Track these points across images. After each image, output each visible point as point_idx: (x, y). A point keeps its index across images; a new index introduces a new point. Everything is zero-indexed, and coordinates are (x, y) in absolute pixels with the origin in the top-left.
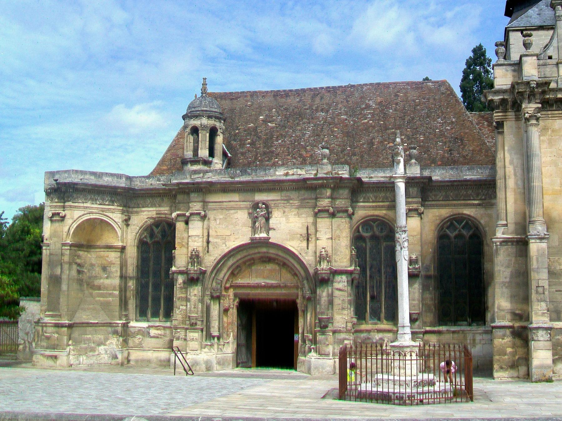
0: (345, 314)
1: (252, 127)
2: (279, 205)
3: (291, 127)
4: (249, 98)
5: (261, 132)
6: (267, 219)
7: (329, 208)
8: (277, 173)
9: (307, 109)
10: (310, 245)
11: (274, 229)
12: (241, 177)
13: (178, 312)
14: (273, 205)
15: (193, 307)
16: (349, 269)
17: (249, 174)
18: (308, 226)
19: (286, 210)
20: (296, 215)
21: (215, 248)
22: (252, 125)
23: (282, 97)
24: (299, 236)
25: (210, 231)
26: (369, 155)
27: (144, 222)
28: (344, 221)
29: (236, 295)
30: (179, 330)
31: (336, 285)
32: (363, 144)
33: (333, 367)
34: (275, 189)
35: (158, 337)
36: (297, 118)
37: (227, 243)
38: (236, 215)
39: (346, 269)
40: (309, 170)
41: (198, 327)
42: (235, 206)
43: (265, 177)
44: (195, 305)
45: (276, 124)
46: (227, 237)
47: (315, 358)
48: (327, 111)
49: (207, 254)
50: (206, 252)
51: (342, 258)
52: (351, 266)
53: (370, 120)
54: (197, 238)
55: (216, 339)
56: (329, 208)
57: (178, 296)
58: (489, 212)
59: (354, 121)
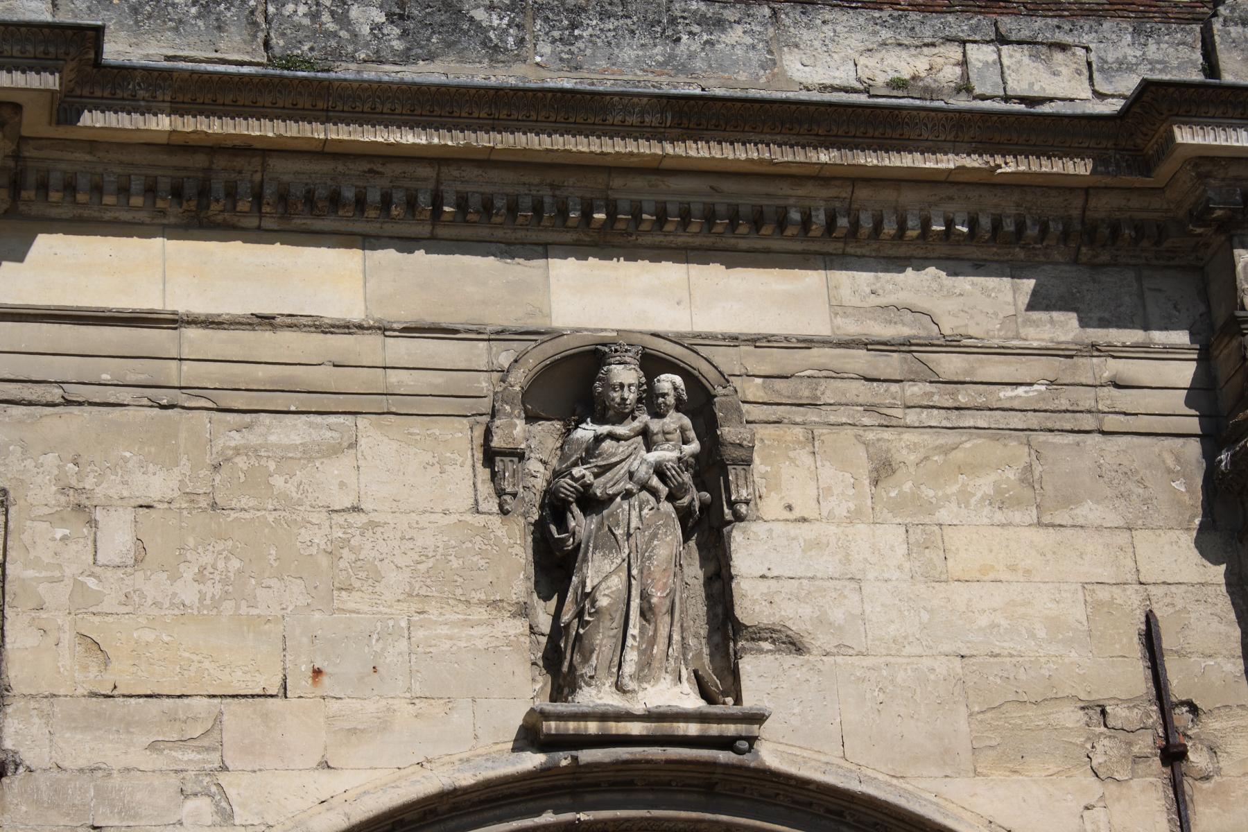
2: (830, 391)
11: (795, 646)
14: (753, 389)
18: (1150, 619)
19: (904, 447)
20: (1017, 503)
24: (1071, 718)
34: (782, 223)
38: (336, 469)
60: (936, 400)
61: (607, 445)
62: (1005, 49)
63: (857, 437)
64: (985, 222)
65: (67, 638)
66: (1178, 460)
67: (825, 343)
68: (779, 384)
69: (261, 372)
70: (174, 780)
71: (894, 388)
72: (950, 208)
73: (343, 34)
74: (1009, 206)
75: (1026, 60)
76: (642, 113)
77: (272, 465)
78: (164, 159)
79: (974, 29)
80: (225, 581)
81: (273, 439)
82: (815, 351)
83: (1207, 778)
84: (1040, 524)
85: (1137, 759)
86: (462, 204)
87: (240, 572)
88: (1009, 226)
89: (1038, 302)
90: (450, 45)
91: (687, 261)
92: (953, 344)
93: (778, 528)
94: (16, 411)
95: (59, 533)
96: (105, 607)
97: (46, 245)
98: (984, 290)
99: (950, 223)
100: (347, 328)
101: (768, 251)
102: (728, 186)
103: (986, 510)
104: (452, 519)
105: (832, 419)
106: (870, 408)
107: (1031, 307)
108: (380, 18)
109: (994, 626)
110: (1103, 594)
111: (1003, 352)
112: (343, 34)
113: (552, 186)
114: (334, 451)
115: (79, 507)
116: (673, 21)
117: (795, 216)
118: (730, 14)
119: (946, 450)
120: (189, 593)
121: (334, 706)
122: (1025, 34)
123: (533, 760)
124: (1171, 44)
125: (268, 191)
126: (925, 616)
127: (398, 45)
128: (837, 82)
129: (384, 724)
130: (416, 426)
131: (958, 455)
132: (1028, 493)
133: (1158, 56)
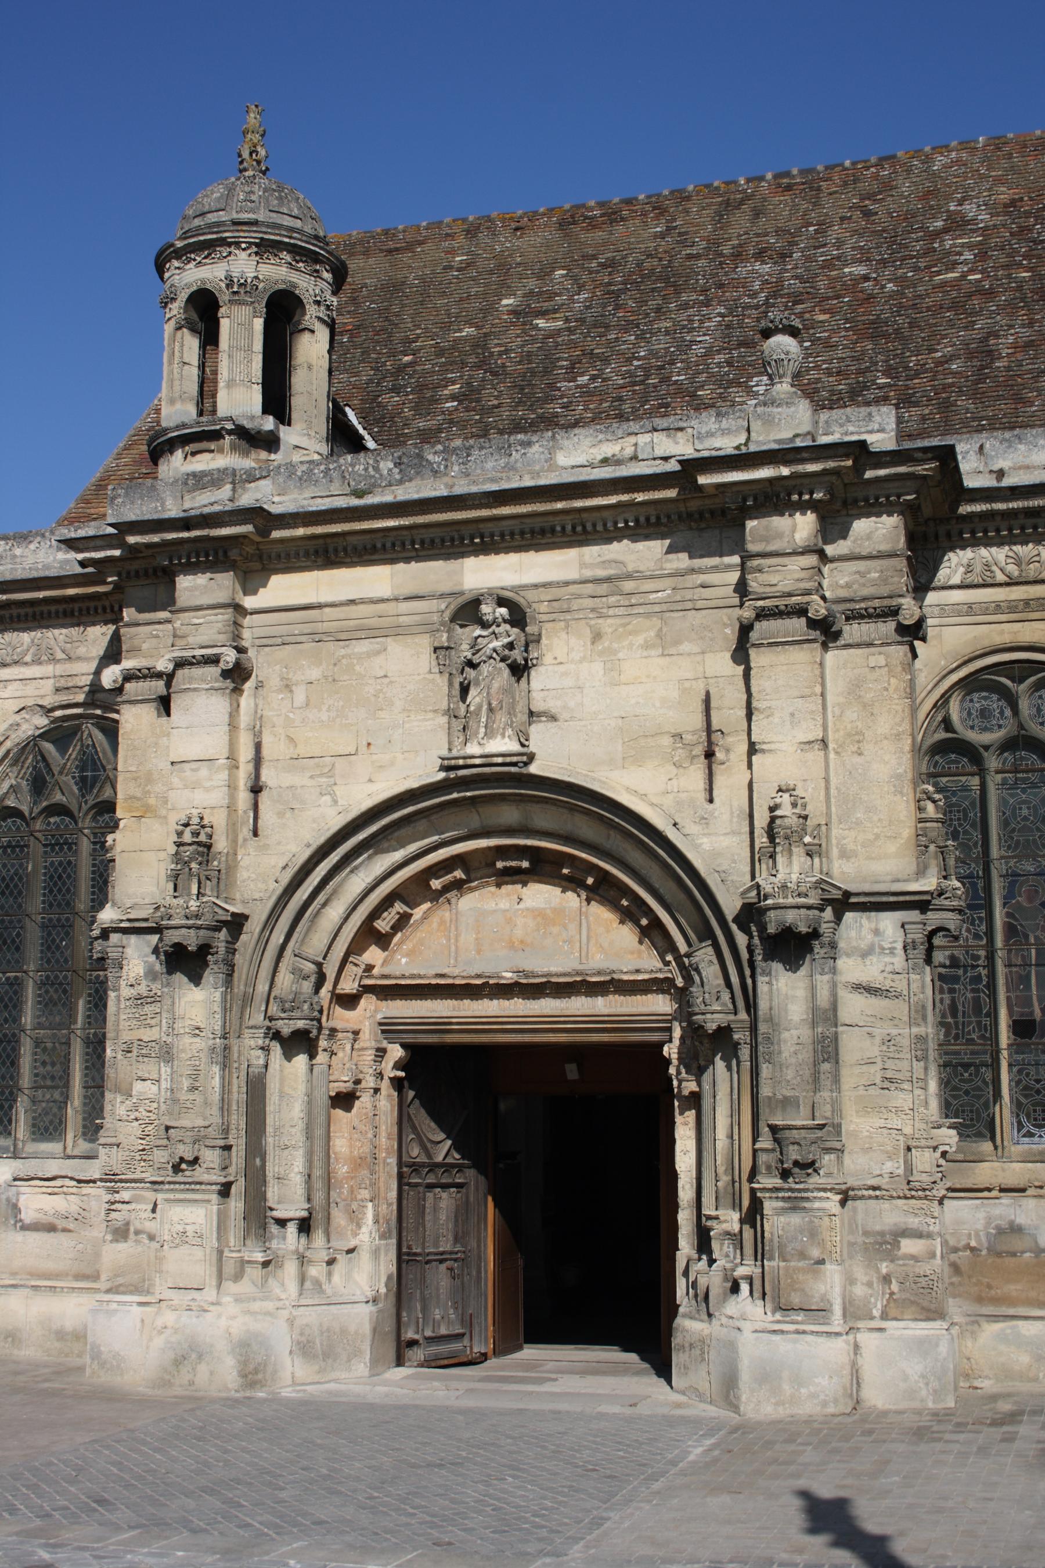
0: (898, 1110)
1: (464, 339)
3: (628, 326)
4: (461, 240)
5: (507, 352)
7: (806, 599)
8: (562, 459)
9: (697, 257)
10: (719, 781)
11: (553, 718)
13: (121, 1111)
14: (544, 607)
15: (186, 1084)
17: (435, 473)
18: (708, 694)
19: (607, 625)
21: (288, 814)
22: (468, 331)
23: (593, 224)
24: (666, 741)
25: (267, 740)
26: (976, 395)
28: (881, 660)
29: (389, 1029)
30: (125, 1195)
31: (850, 969)
32: (948, 359)
33: (846, 1372)
34: (553, 531)
35: (51, 1228)
36: (653, 290)
37: (339, 791)
38: (379, 660)
40: (710, 434)
41: (206, 1178)
42: (374, 622)
43: (509, 479)
44: (195, 1077)
45: (567, 320)
47: (759, 1326)
48: (784, 256)
49: (253, 842)
50: (245, 832)
51: (877, 837)
52: (921, 872)
53: (971, 271)
54: (204, 771)
55: (292, 1229)
56: (806, 599)
57: (126, 1036)
60: (622, 603)
61: (479, 640)
62: (655, 434)
63: (587, 624)
64: (642, 519)
65: (283, 737)
66: (729, 619)
67: (574, 583)
68: (555, 604)
69: (352, 623)
70: (318, 790)
71: (604, 599)
72: (626, 515)
73: (377, 476)
74: (652, 511)
75: (664, 438)
76: (480, 499)
77: (355, 661)
78: (309, 543)
79: (642, 427)
80: (337, 711)
81: (356, 650)
82: (571, 587)
83: (723, 763)
84: (663, 655)
85: (694, 757)
86: (422, 543)
87: (343, 706)
88: (653, 520)
89: (670, 550)
90: (418, 473)
91: (520, 551)
92: (629, 577)
93: (550, 668)
94: (267, 649)
95: (280, 696)
96: (296, 724)
97: (276, 580)
98: (649, 548)
99: (626, 522)
101: (554, 543)
102: (527, 521)
103: (640, 652)
104: (421, 677)
105: (577, 617)
106: (593, 610)
107: (668, 552)
108: (391, 465)
109: (638, 703)
110: (687, 684)
111: (652, 577)
112: (377, 476)
113: (458, 531)
114: (378, 653)
115: (287, 686)
116: (510, 446)
117: (558, 528)
118: (534, 438)
119: (624, 625)
120: (324, 716)
121: (375, 757)
122: (665, 425)
123: (442, 775)
124: (733, 419)
125: (349, 549)
126: (608, 701)
127: (398, 477)
128: (578, 464)
129: (392, 763)
130: (409, 639)
131: (630, 627)
132: (659, 641)
133: (726, 427)
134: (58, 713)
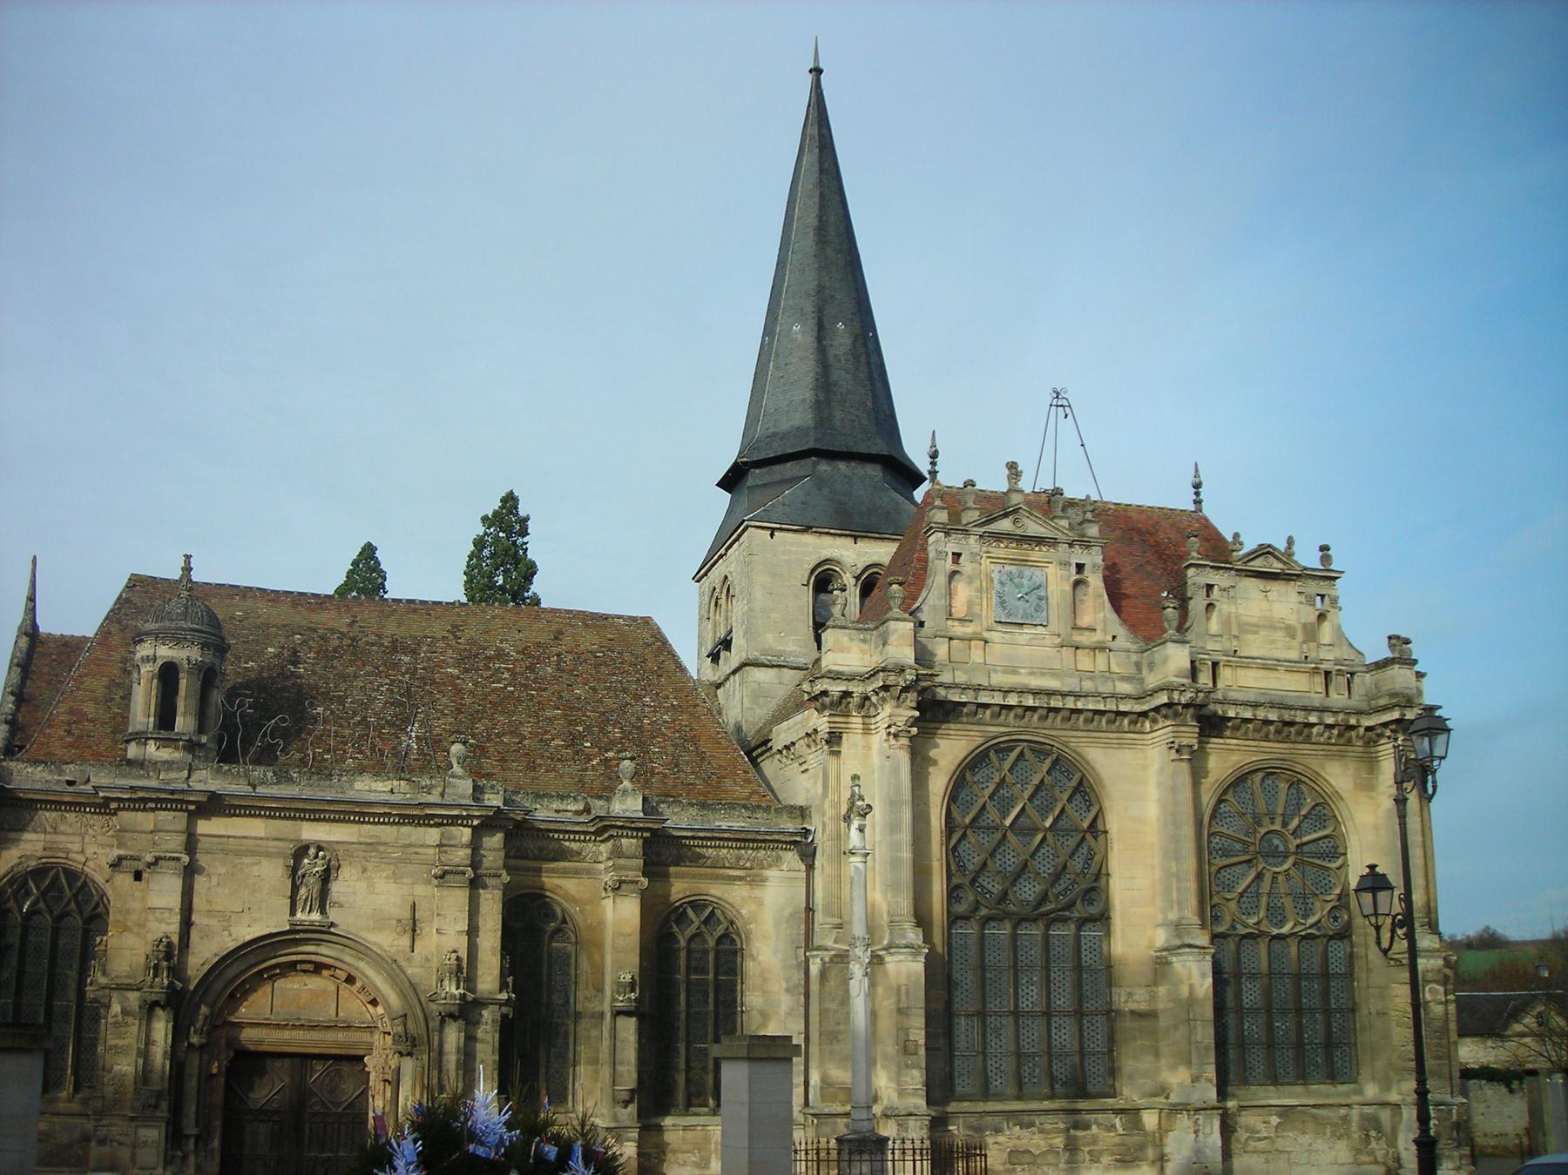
6: (326, 877)
10: (417, 943)
11: (341, 906)
12: (276, 787)
16: (499, 997)
19: (370, 866)
24: (394, 922)
27: (10, 865)
28: (491, 896)
36: (351, 661)
38: (257, 867)
39: (491, 996)
46: (233, 916)
52: (501, 991)
54: (167, 914)
58: (757, 893)
59: (476, 684)
100: (262, 839)
114: (256, 864)
129: (261, 919)
134: (44, 860)
